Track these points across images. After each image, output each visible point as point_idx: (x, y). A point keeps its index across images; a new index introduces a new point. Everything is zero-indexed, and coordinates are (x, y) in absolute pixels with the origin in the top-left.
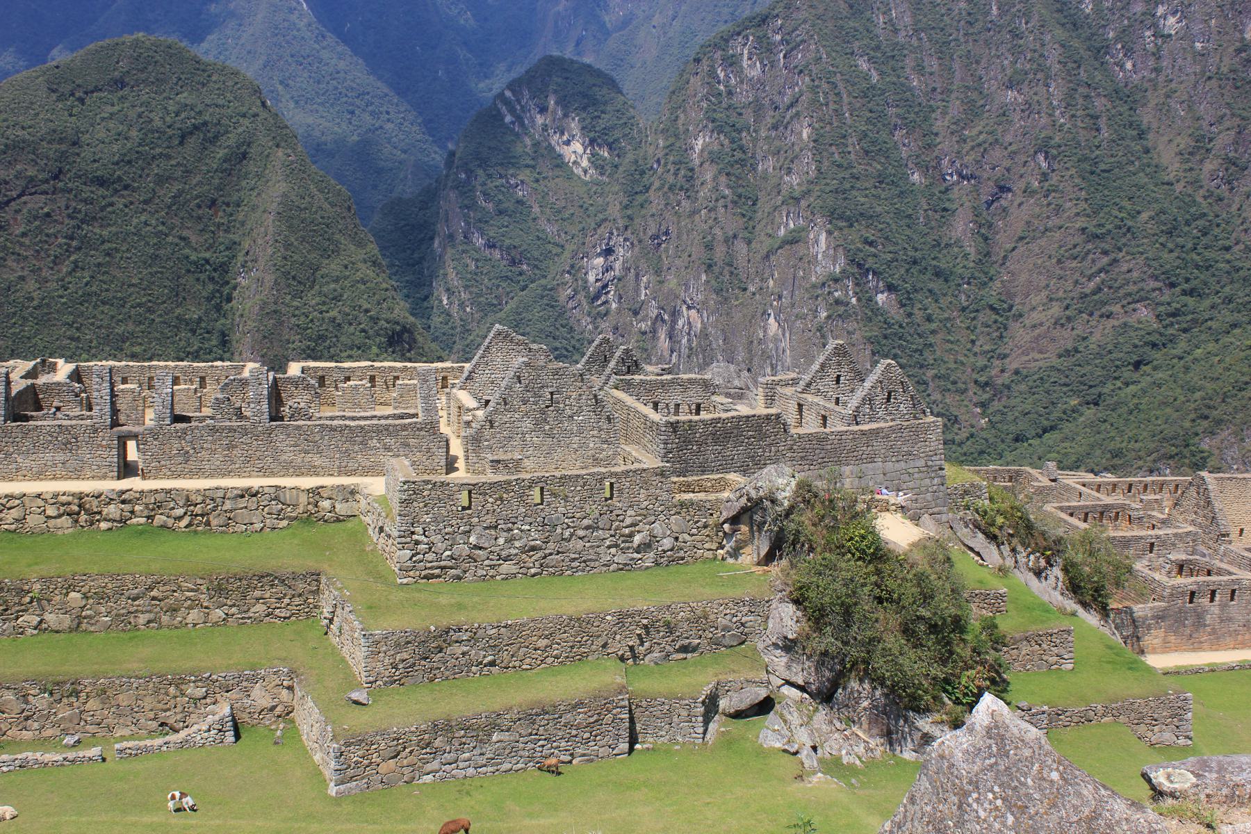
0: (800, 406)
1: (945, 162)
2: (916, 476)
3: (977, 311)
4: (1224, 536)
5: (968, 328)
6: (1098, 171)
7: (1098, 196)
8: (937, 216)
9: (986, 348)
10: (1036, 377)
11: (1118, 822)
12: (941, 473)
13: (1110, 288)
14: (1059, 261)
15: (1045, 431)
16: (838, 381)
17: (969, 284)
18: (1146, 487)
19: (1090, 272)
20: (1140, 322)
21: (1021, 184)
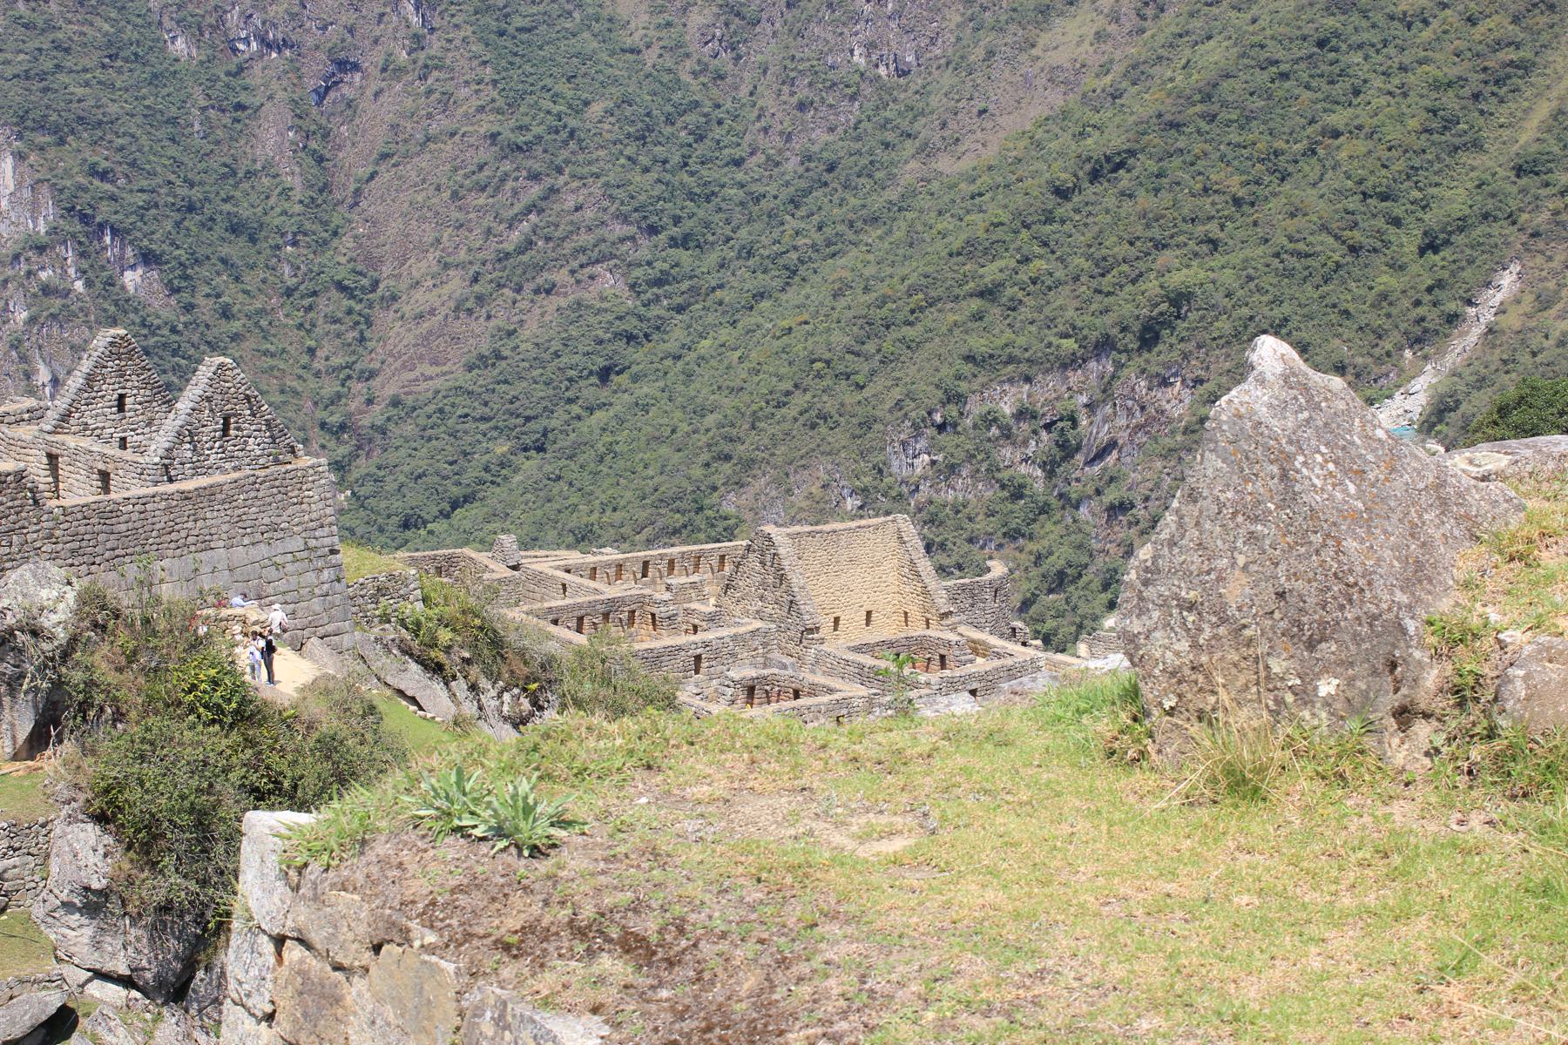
0: (52, 458)
1: (233, 18)
2: (289, 568)
3: (315, 294)
4: (810, 631)
5: (300, 326)
6: (511, 30)
7: (515, 74)
8: (227, 120)
9: (337, 361)
10: (431, 408)
11: (1467, 489)
12: (333, 559)
13: (548, 239)
14: (455, 196)
15: (455, 505)
16: (121, 405)
17: (295, 244)
18: (671, 563)
19: (511, 213)
20: (603, 299)
21: (376, 57)
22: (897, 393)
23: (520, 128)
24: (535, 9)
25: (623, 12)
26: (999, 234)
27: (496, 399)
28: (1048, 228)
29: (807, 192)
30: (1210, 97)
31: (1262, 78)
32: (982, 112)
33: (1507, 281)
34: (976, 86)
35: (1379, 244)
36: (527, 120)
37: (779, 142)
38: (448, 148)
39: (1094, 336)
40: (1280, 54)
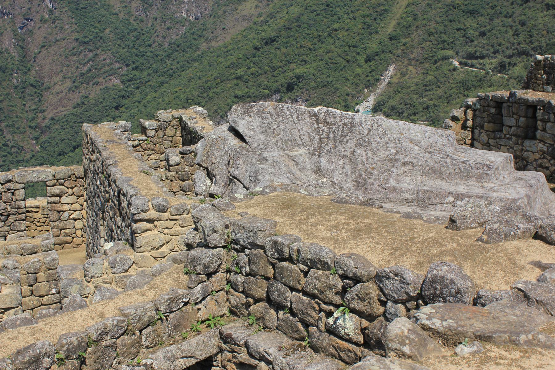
3: (24, 88)
6: (80, 8)
7: (82, 21)
9: (33, 107)
10: (64, 120)
13: (96, 69)
14: (66, 57)
15: (75, 148)
17: (17, 73)
19: (84, 62)
20: (114, 86)
21: (39, 17)
22: (215, 108)
23: (85, 37)
24: (86, 2)
25: (112, 2)
26: (240, 61)
27: (84, 116)
28: (254, 59)
29: (172, 53)
30: (298, 21)
31: (313, 15)
32: (223, 29)
33: (392, 69)
34: (221, 22)
35: (354, 60)
36: (87, 34)
37: (161, 39)
38: (63, 43)
39: (273, 89)
40: (317, 9)
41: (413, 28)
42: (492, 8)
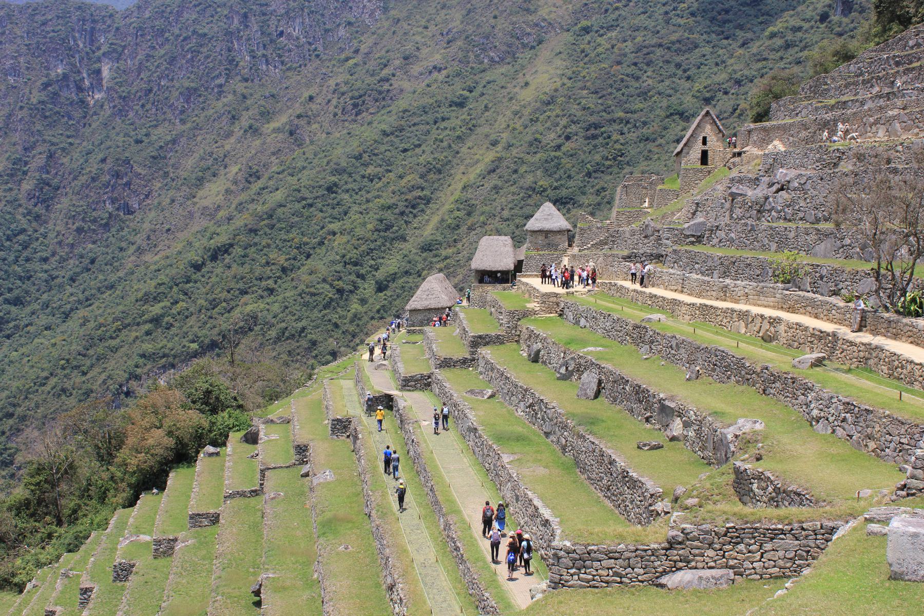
22: (103, 376)
26: (162, 289)
30: (271, 216)
31: (298, 206)
32: (169, 230)
37: (67, 250)
39: (207, 341)
40: (308, 195)
41: (464, 228)
42: (598, 193)
